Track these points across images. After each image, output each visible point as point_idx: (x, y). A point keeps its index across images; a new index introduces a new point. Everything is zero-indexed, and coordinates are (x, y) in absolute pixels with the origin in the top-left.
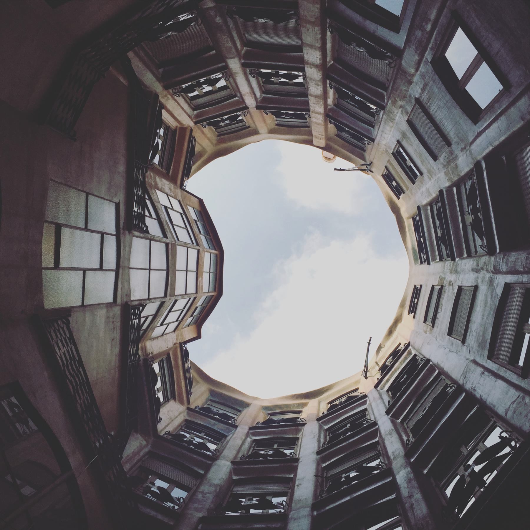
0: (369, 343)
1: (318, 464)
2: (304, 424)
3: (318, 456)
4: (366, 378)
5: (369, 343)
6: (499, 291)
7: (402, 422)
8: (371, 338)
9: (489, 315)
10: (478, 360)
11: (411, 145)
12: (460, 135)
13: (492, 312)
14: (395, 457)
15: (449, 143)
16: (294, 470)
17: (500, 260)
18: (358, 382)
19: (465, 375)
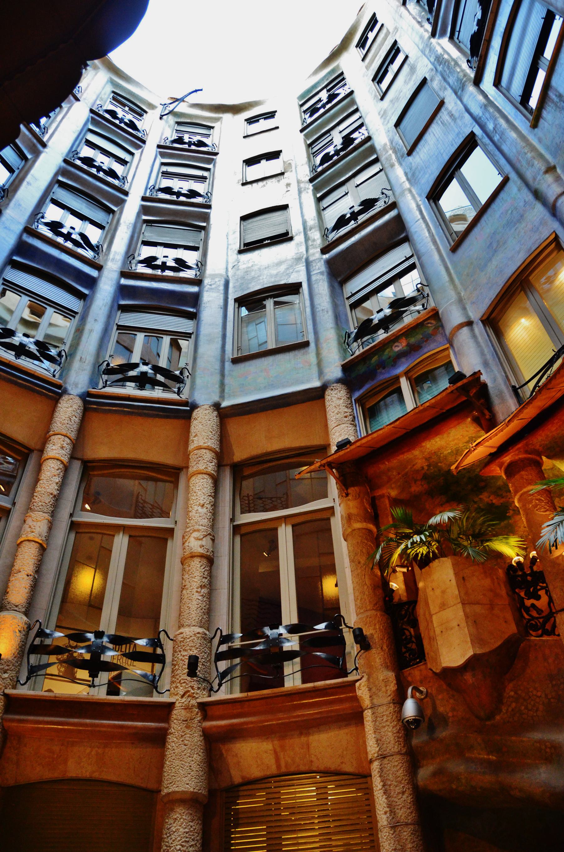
0: (196, 91)
1: (56, 174)
2: (77, 100)
3: (63, 164)
4: (161, 118)
5: (196, 91)
6: (292, 279)
7: (145, 221)
8: (201, 90)
9: (271, 276)
10: (231, 285)
11: (406, 82)
12: (417, 173)
13: (273, 280)
14: (113, 259)
15: (410, 153)
16: (37, 154)
17: (319, 269)
18: (152, 107)
19: (213, 276)
